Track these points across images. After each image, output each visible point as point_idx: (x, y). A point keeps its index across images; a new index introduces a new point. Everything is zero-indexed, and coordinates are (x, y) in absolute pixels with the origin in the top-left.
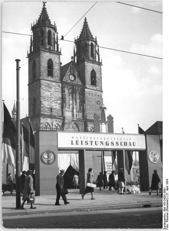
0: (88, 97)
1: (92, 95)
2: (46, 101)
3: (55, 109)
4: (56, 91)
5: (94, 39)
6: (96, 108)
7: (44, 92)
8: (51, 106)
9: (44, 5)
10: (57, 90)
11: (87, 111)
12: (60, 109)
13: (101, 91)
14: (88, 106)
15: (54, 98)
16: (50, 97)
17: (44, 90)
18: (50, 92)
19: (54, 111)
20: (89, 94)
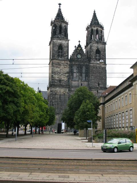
3: (63, 80)
4: (65, 67)
9: (60, 7)
13: (105, 65)
19: (62, 82)
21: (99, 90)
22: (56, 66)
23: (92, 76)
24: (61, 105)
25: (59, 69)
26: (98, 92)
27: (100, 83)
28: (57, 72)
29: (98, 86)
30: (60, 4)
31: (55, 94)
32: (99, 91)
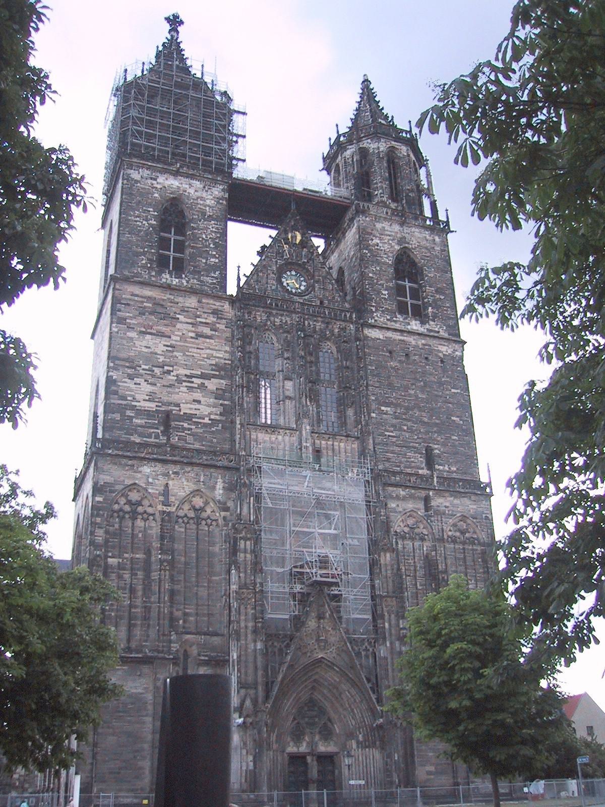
0: (386, 367)
1: (403, 359)
2: (136, 380)
3: (188, 417)
4: (199, 335)
5: (406, 132)
6: (431, 417)
7: (132, 339)
8: (170, 404)
10: (207, 331)
11: (382, 435)
12: (218, 417)
14: (383, 408)
15: (186, 367)
16: (161, 359)
17: (130, 328)
18: (170, 337)
19: (184, 429)
20: (390, 352)
21: (439, 492)
22: (140, 320)
23: (387, 405)
24: (172, 593)
25: (165, 341)
26: (427, 508)
27: (437, 450)
28: (147, 360)
29: (424, 472)
30: (175, 22)
31: (127, 508)
32: (438, 502)
